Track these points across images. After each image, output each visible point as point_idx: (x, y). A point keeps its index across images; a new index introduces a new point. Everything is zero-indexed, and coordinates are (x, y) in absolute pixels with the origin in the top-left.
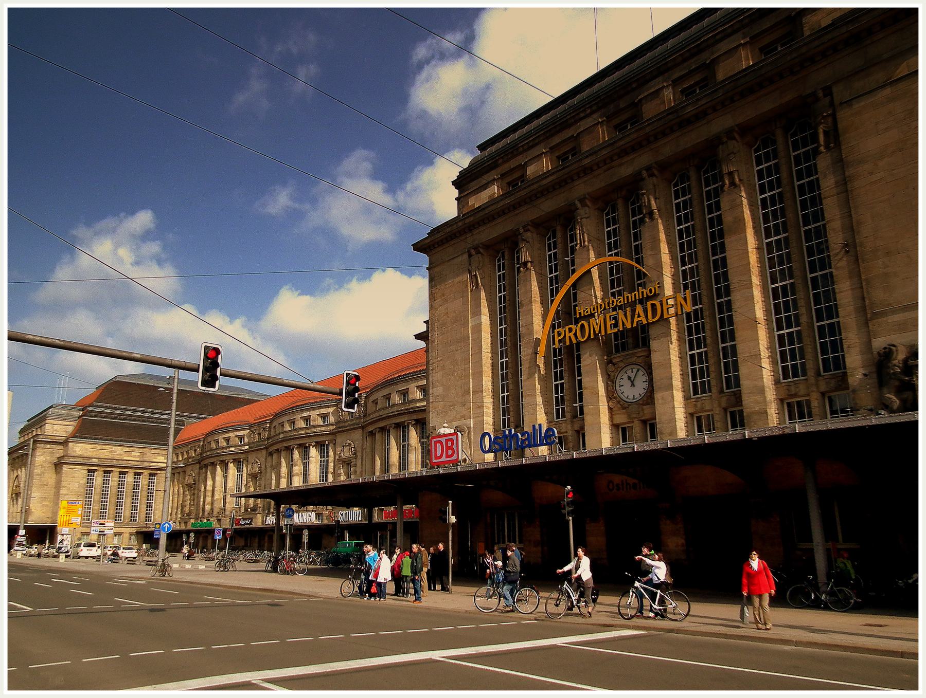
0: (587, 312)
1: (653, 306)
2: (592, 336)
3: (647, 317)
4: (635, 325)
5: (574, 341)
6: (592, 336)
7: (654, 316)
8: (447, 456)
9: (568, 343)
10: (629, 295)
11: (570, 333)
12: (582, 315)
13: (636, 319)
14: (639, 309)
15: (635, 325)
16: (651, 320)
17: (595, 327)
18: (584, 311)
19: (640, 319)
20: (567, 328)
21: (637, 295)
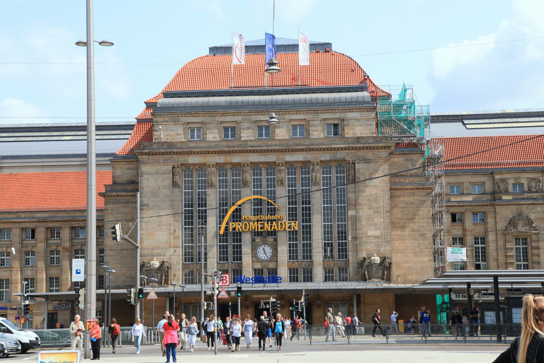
0: (249, 219)
1: (281, 224)
2: (251, 230)
3: (278, 229)
4: (272, 230)
5: (241, 230)
6: (251, 230)
7: (281, 228)
8: (223, 283)
9: (237, 230)
10: (271, 216)
11: (238, 226)
12: (246, 219)
13: (273, 228)
14: (274, 223)
15: (272, 230)
16: (279, 229)
17: (252, 226)
18: (247, 218)
19: (274, 228)
20: (237, 223)
21: (273, 217)
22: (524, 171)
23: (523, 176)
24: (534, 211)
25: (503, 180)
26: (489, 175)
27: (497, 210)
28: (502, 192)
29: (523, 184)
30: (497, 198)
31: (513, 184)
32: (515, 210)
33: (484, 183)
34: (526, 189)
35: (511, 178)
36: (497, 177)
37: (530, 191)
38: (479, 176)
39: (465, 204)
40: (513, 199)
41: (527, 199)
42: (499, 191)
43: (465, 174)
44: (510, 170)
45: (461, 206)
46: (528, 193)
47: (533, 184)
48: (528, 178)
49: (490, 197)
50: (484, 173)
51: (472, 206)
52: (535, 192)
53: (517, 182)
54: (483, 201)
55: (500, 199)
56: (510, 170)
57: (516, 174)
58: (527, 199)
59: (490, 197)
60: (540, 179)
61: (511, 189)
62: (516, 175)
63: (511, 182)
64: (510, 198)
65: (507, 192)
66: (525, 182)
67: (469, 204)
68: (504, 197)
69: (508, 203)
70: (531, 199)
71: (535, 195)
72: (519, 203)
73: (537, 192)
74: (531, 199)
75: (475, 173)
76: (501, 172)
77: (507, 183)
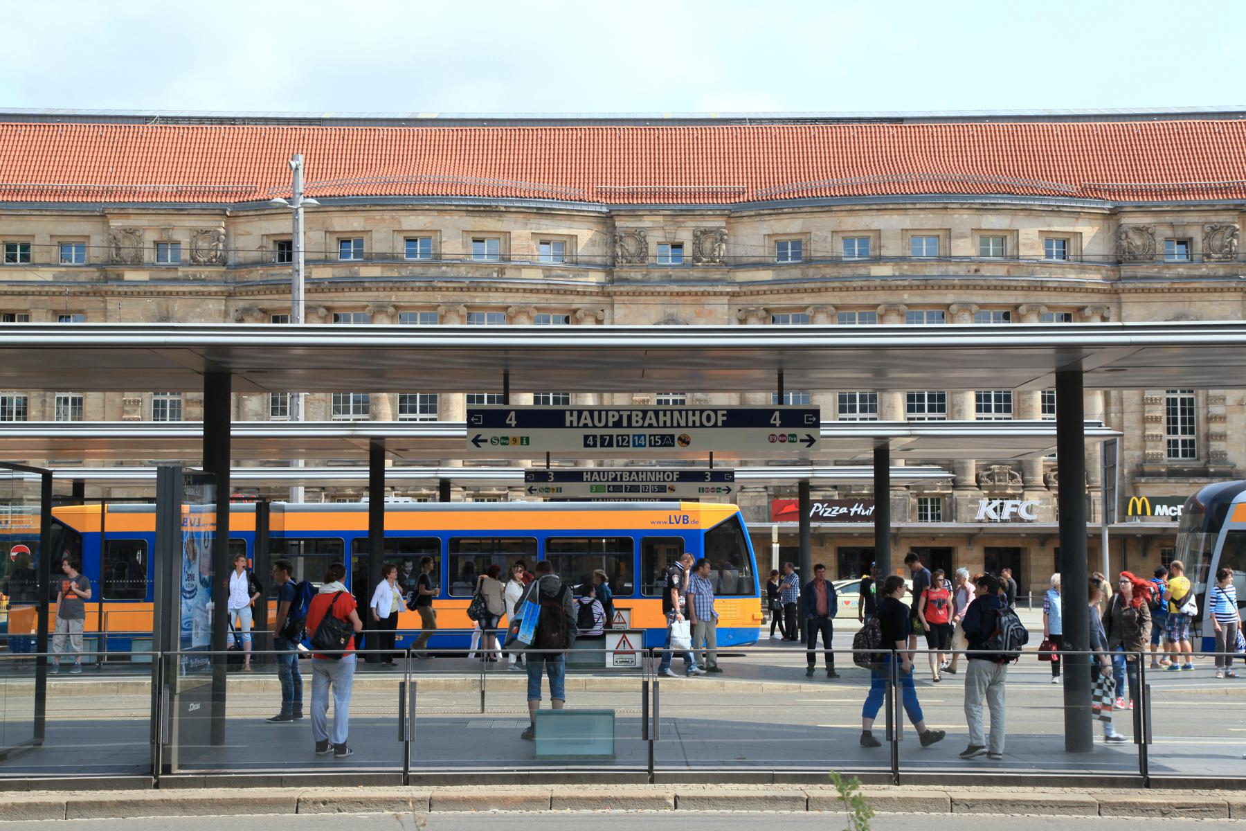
22: (180, 210)
23: (180, 224)
24: (198, 310)
25: (130, 232)
26: (99, 219)
27: (109, 307)
28: (125, 261)
29: (179, 243)
30: (113, 276)
31: (157, 244)
32: (154, 307)
33: (88, 237)
34: (185, 255)
35: (149, 228)
36: (116, 223)
37: (195, 262)
38: (75, 219)
39: (27, 289)
40: (152, 280)
41: (186, 280)
42: (118, 259)
43: (38, 213)
44: (144, 209)
45: (20, 294)
46: (191, 265)
47: (204, 244)
48: (191, 229)
49: (97, 274)
50: (87, 214)
51: (47, 294)
52: (205, 264)
53: (165, 237)
54: (79, 282)
55: (119, 278)
56: (144, 209)
57: (162, 218)
58: (186, 280)
59: (97, 274)
60: (219, 234)
61: (149, 256)
62: (162, 221)
63: (150, 237)
64: (143, 276)
65: (137, 263)
66: (183, 238)
67: (39, 289)
68: (130, 275)
69: (136, 292)
70: (196, 280)
71: (205, 272)
72: (159, 289)
73: (209, 263)
74: (196, 280)
75: (64, 211)
76: (123, 210)
77: (140, 240)
